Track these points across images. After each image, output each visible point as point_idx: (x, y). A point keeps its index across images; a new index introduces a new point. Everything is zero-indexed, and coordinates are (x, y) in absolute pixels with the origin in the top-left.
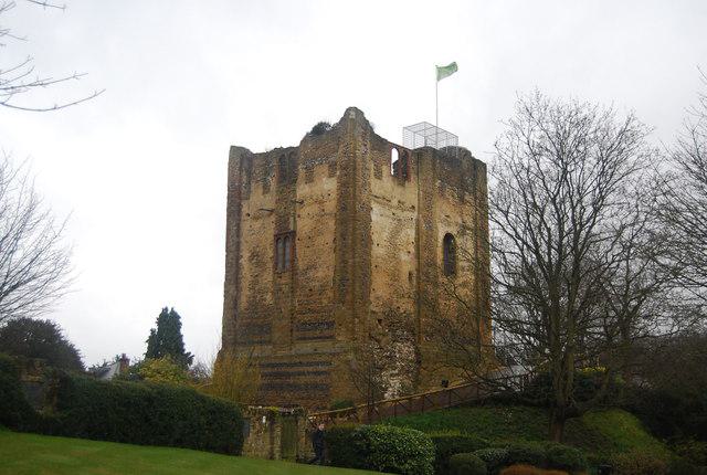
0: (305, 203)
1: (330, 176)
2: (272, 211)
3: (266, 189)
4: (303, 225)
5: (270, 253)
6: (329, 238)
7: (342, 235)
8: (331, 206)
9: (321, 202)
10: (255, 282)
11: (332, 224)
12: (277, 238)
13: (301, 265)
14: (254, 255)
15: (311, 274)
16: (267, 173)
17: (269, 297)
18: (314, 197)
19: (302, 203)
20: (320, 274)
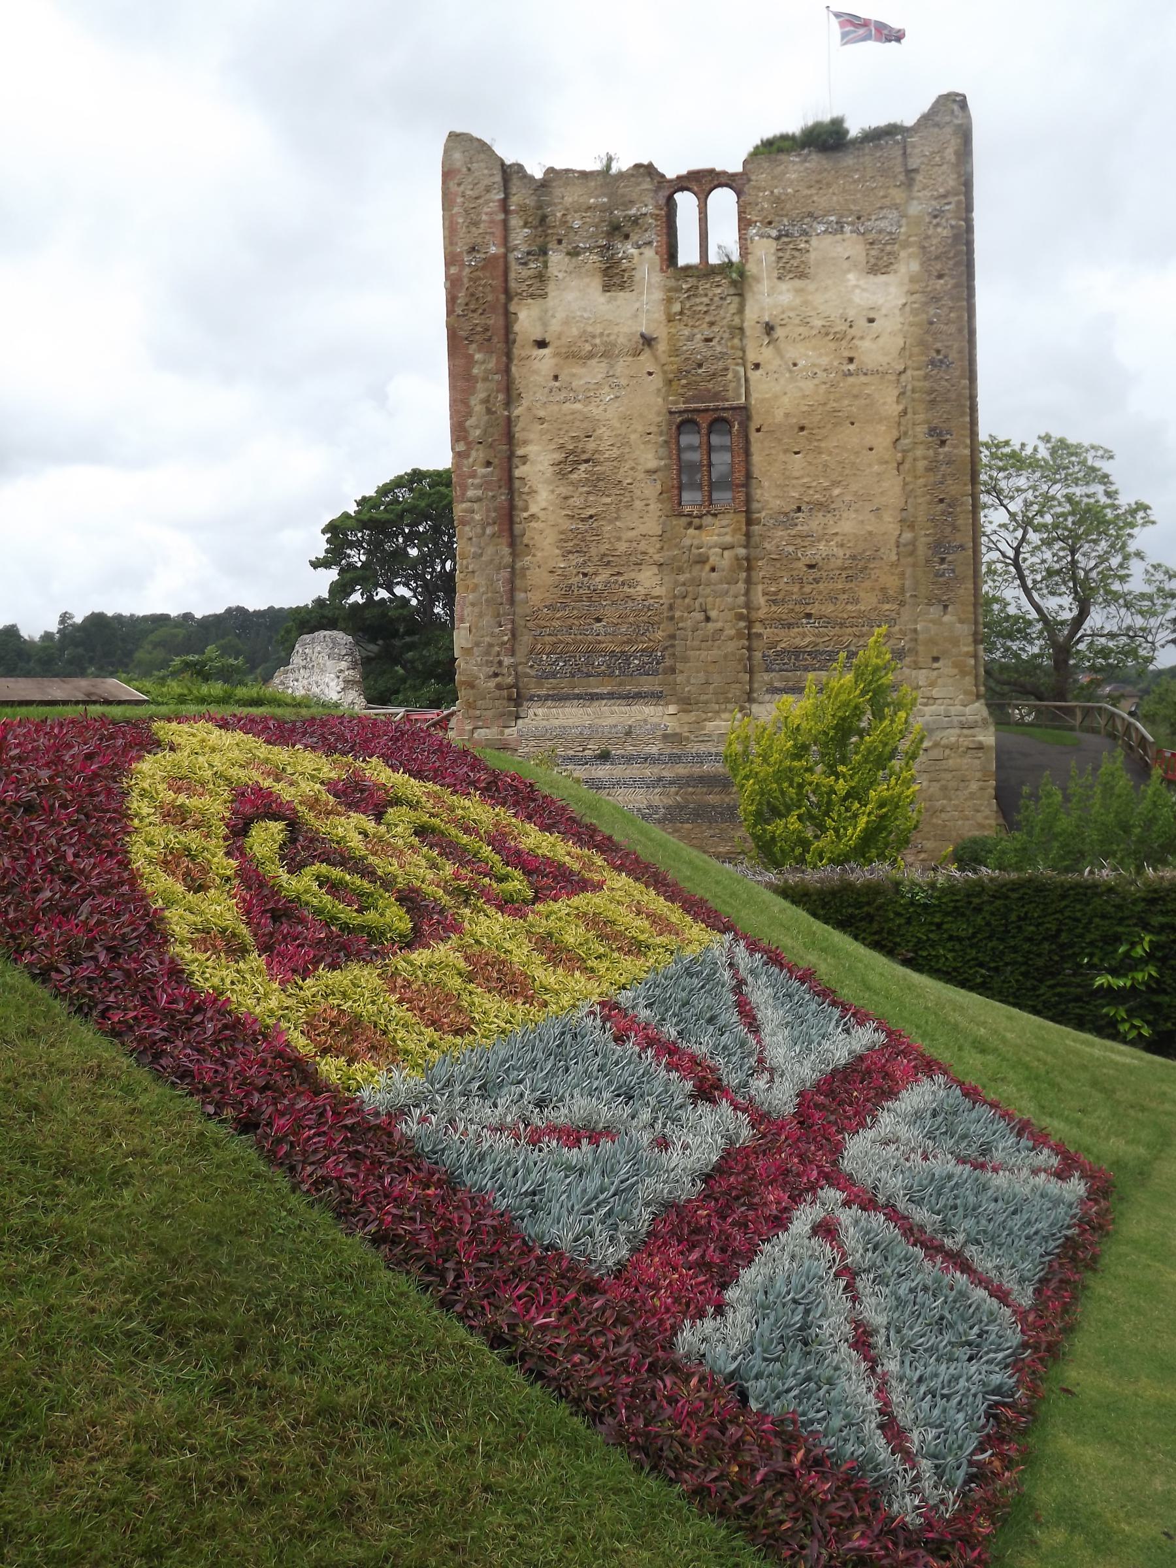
0: (779, 332)
1: (877, 267)
2: (648, 341)
3: (614, 277)
4: (777, 387)
5: (649, 458)
6: (881, 437)
7: (932, 431)
8: (883, 346)
9: (839, 338)
10: (576, 543)
11: (888, 403)
12: (684, 423)
13: (769, 497)
14: (571, 460)
15: (814, 523)
16: (617, 230)
17: (648, 581)
18: (818, 323)
19: (769, 329)
20: (848, 525)
